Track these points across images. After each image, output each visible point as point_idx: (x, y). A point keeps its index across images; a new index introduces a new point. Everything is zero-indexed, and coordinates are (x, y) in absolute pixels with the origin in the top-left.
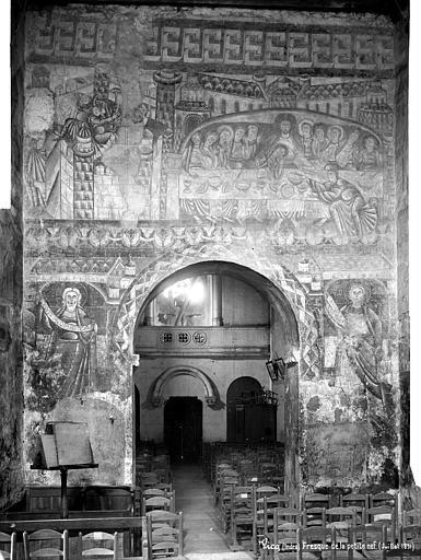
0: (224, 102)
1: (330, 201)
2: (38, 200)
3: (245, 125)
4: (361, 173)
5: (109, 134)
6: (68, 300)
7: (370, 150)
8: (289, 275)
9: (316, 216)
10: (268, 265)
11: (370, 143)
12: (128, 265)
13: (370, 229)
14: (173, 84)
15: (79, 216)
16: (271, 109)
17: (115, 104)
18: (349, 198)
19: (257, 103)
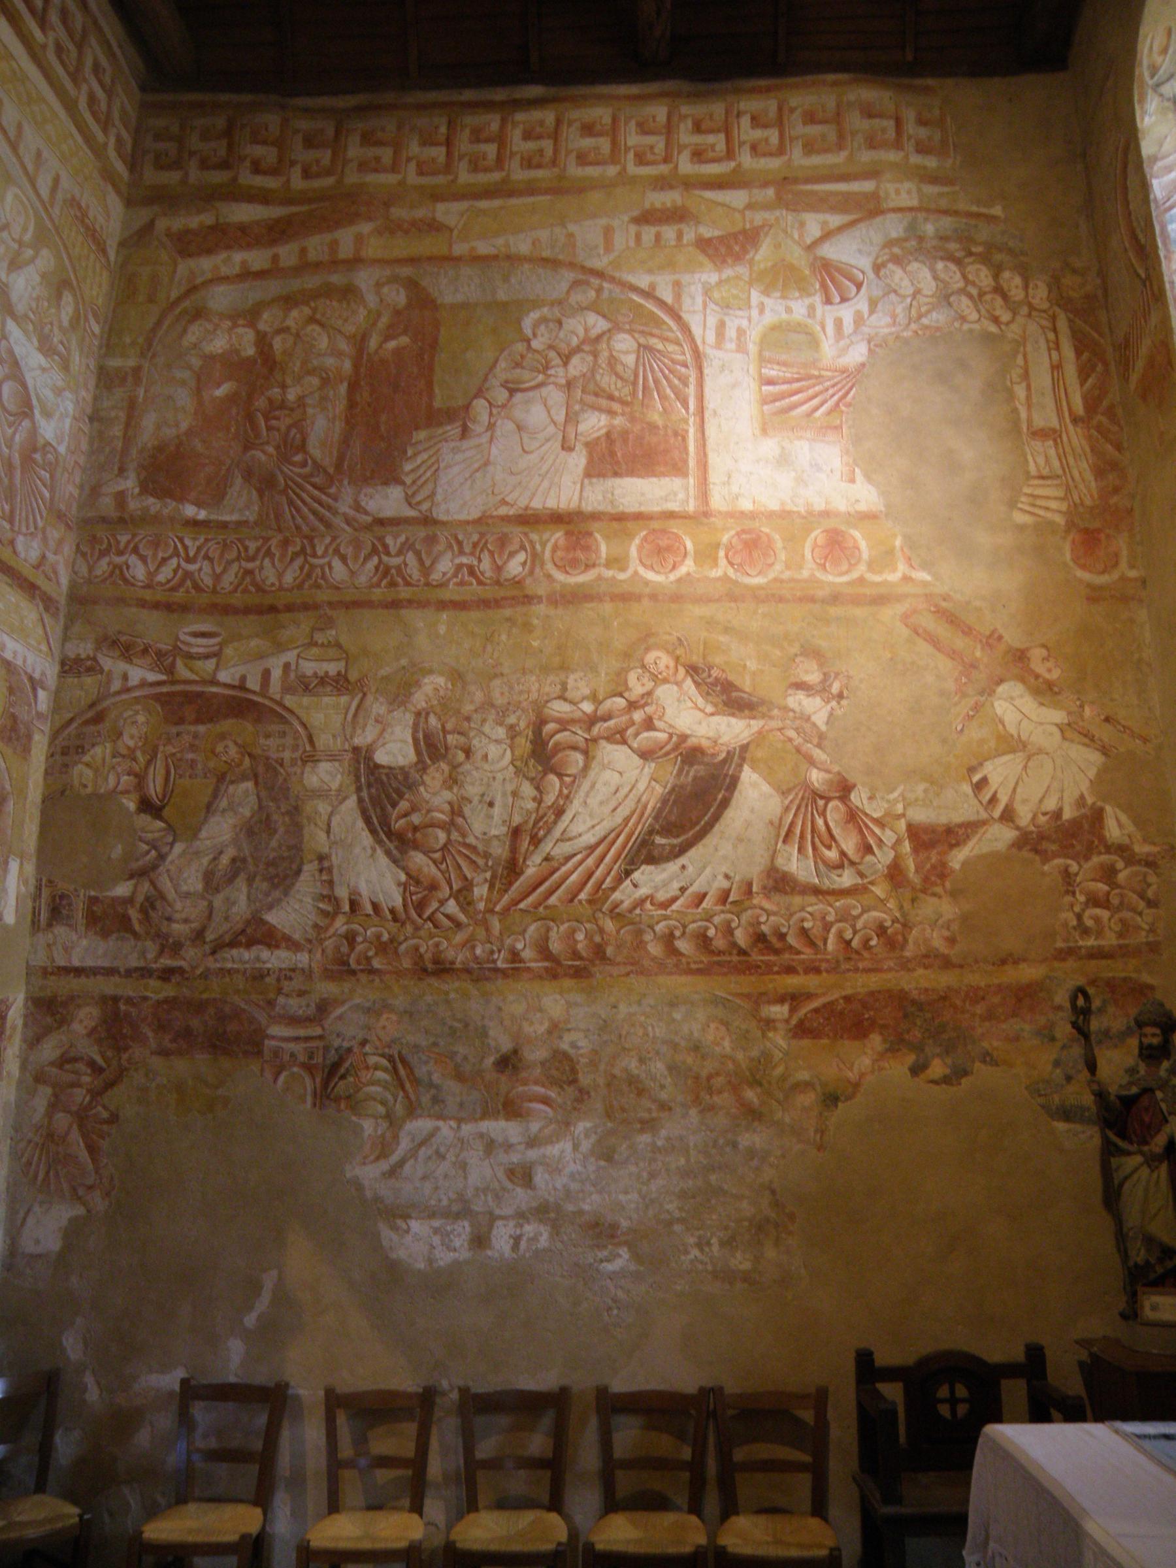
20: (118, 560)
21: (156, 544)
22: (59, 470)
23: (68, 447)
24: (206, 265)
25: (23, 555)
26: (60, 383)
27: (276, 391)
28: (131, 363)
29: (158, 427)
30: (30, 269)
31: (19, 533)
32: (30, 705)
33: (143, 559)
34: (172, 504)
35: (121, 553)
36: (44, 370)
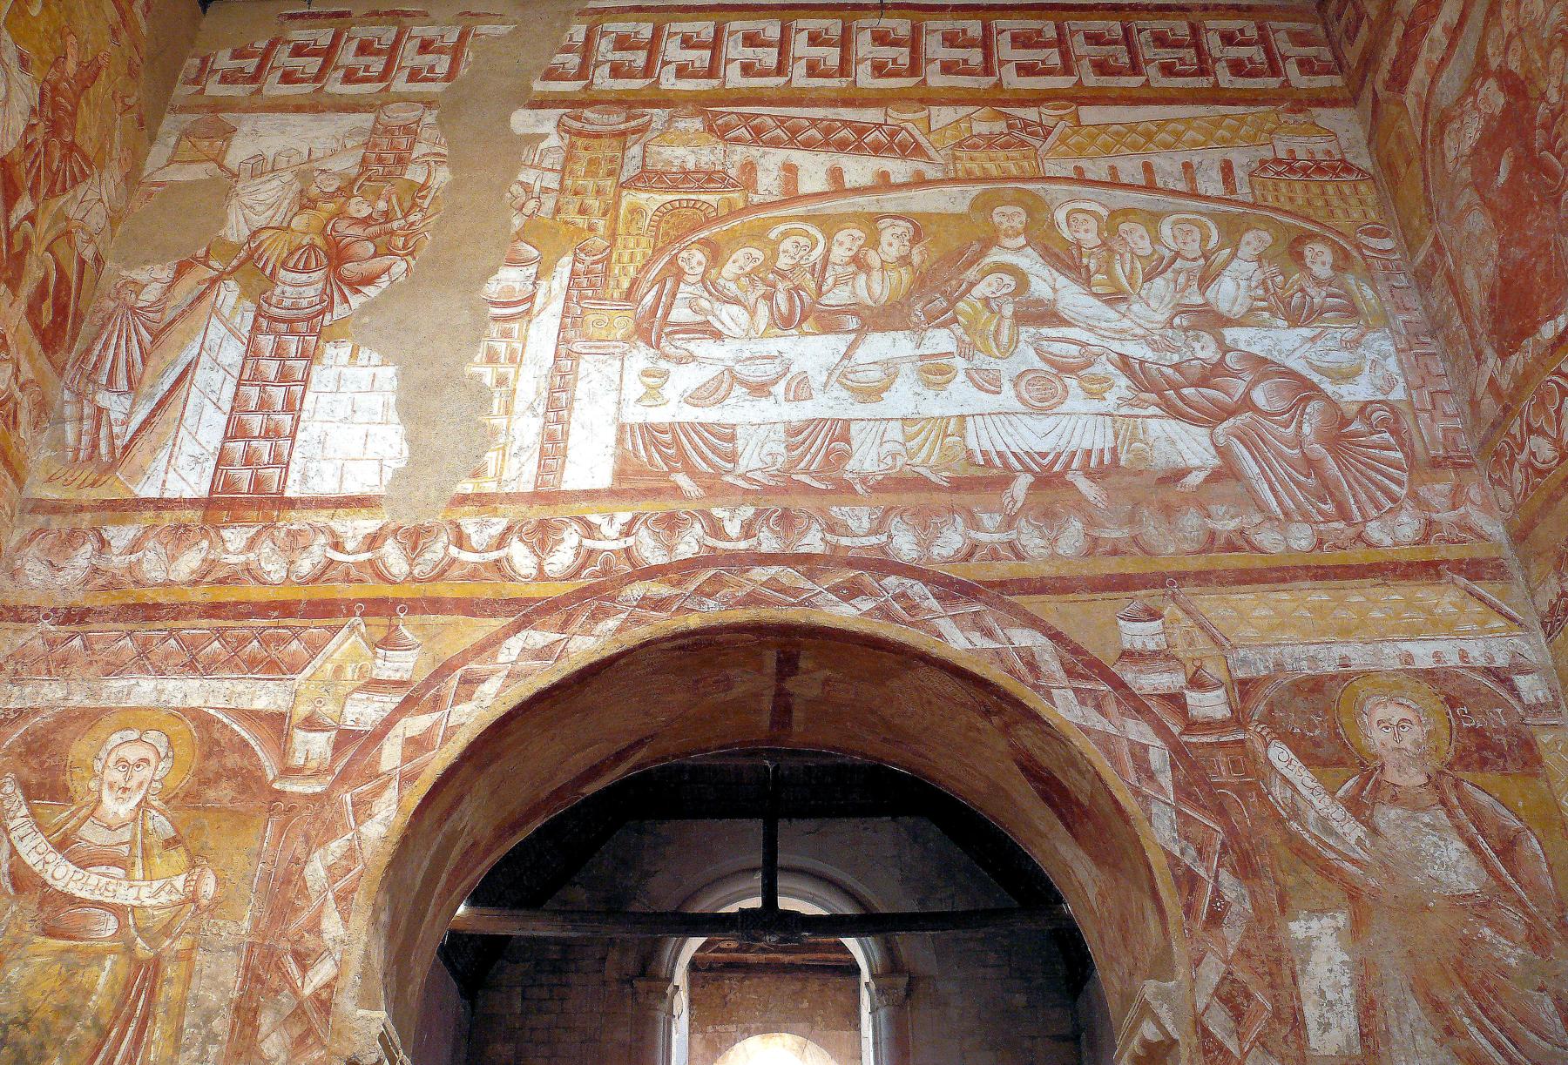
0: (790, 170)
1: (1211, 417)
2: (95, 446)
3: (872, 221)
4: (1306, 332)
5: (386, 261)
6: (117, 776)
7: (1322, 270)
8: (1084, 666)
9: (1161, 458)
10: (988, 633)
11: (1320, 258)
12: (389, 642)
13: (1394, 500)
14: (623, 134)
15: (230, 485)
16: (955, 181)
17: (424, 186)
18: (1280, 405)
19: (899, 169)
20: (1523, 457)
21: (1542, 404)
22: (1407, 422)
23: (1409, 387)
24: (1420, 73)
25: (1388, 541)
26: (1350, 335)
27: (1543, 110)
28: (1429, 240)
29: (1479, 276)
30: (1235, 264)
31: (1366, 520)
32: (1503, 704)
33: (1541, 432)
34: (1528, 343)
35: (1522, 447)
36: (1313, 339)
